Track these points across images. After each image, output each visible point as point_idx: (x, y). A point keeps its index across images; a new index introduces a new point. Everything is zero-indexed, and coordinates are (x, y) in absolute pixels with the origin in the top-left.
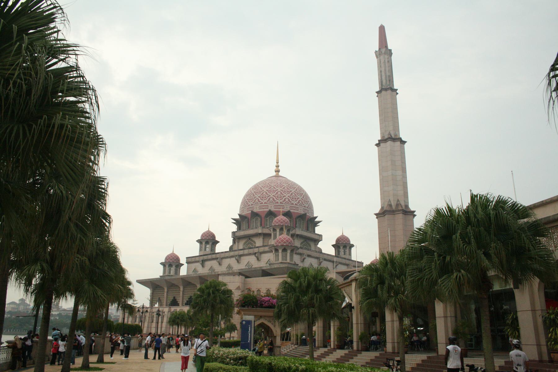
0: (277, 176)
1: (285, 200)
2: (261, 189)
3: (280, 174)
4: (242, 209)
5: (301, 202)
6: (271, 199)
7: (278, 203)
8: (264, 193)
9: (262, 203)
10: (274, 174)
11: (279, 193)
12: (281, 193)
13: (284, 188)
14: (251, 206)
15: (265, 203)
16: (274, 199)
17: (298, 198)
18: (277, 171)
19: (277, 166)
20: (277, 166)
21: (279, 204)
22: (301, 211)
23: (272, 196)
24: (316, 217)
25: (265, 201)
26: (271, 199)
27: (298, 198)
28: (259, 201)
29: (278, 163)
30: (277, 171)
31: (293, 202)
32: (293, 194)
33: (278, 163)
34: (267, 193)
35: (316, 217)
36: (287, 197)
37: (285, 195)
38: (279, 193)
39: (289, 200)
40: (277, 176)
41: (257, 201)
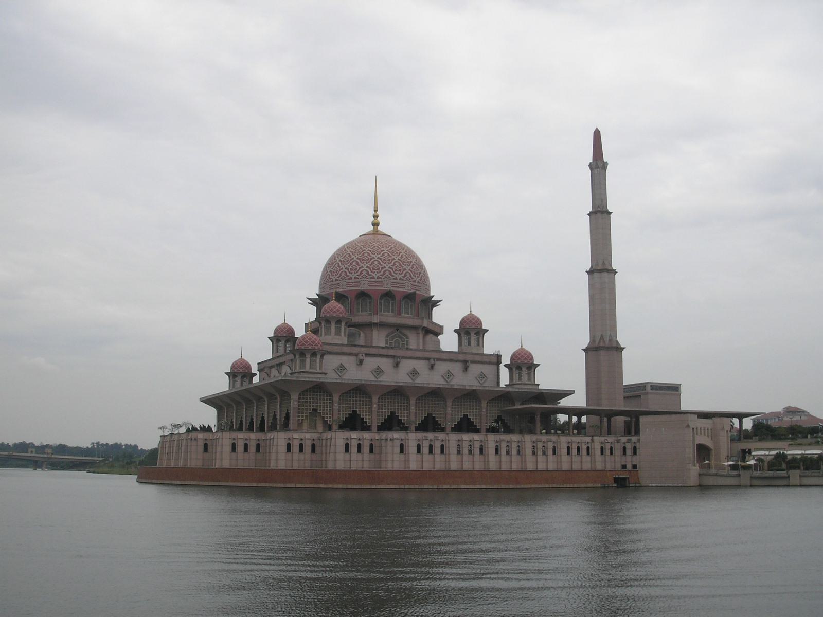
0: (376, 233)
1: (384, 273)
2: (350, 256)
3: (380, 228)
4: (322, 285)
6: (364, 273)
7: (373, 278)
8: (354, 263)
9: (351, 278)
10: (371, 228)
11: (376, 263)
12: (379, 263)
13: (383, 255)
14: (334, 283)
16: (368, 273)
17: (405, 269)
18: (375, 224)
19: (376, 217)
20: (376, 217)
22: (408, 289)
24: (433, 296)
25: (355, 275)
26: (364, 273)
27: (405, 269)
28: (346, 274)
29: (376, 211)
30: (375, 224)
32: (397, 264)
33: (376, 211)
34: (357, 263)
35: (433, 296)
36: (387, 268)
38: (376, 263)
40: (376, 233)
41: (343, 274)
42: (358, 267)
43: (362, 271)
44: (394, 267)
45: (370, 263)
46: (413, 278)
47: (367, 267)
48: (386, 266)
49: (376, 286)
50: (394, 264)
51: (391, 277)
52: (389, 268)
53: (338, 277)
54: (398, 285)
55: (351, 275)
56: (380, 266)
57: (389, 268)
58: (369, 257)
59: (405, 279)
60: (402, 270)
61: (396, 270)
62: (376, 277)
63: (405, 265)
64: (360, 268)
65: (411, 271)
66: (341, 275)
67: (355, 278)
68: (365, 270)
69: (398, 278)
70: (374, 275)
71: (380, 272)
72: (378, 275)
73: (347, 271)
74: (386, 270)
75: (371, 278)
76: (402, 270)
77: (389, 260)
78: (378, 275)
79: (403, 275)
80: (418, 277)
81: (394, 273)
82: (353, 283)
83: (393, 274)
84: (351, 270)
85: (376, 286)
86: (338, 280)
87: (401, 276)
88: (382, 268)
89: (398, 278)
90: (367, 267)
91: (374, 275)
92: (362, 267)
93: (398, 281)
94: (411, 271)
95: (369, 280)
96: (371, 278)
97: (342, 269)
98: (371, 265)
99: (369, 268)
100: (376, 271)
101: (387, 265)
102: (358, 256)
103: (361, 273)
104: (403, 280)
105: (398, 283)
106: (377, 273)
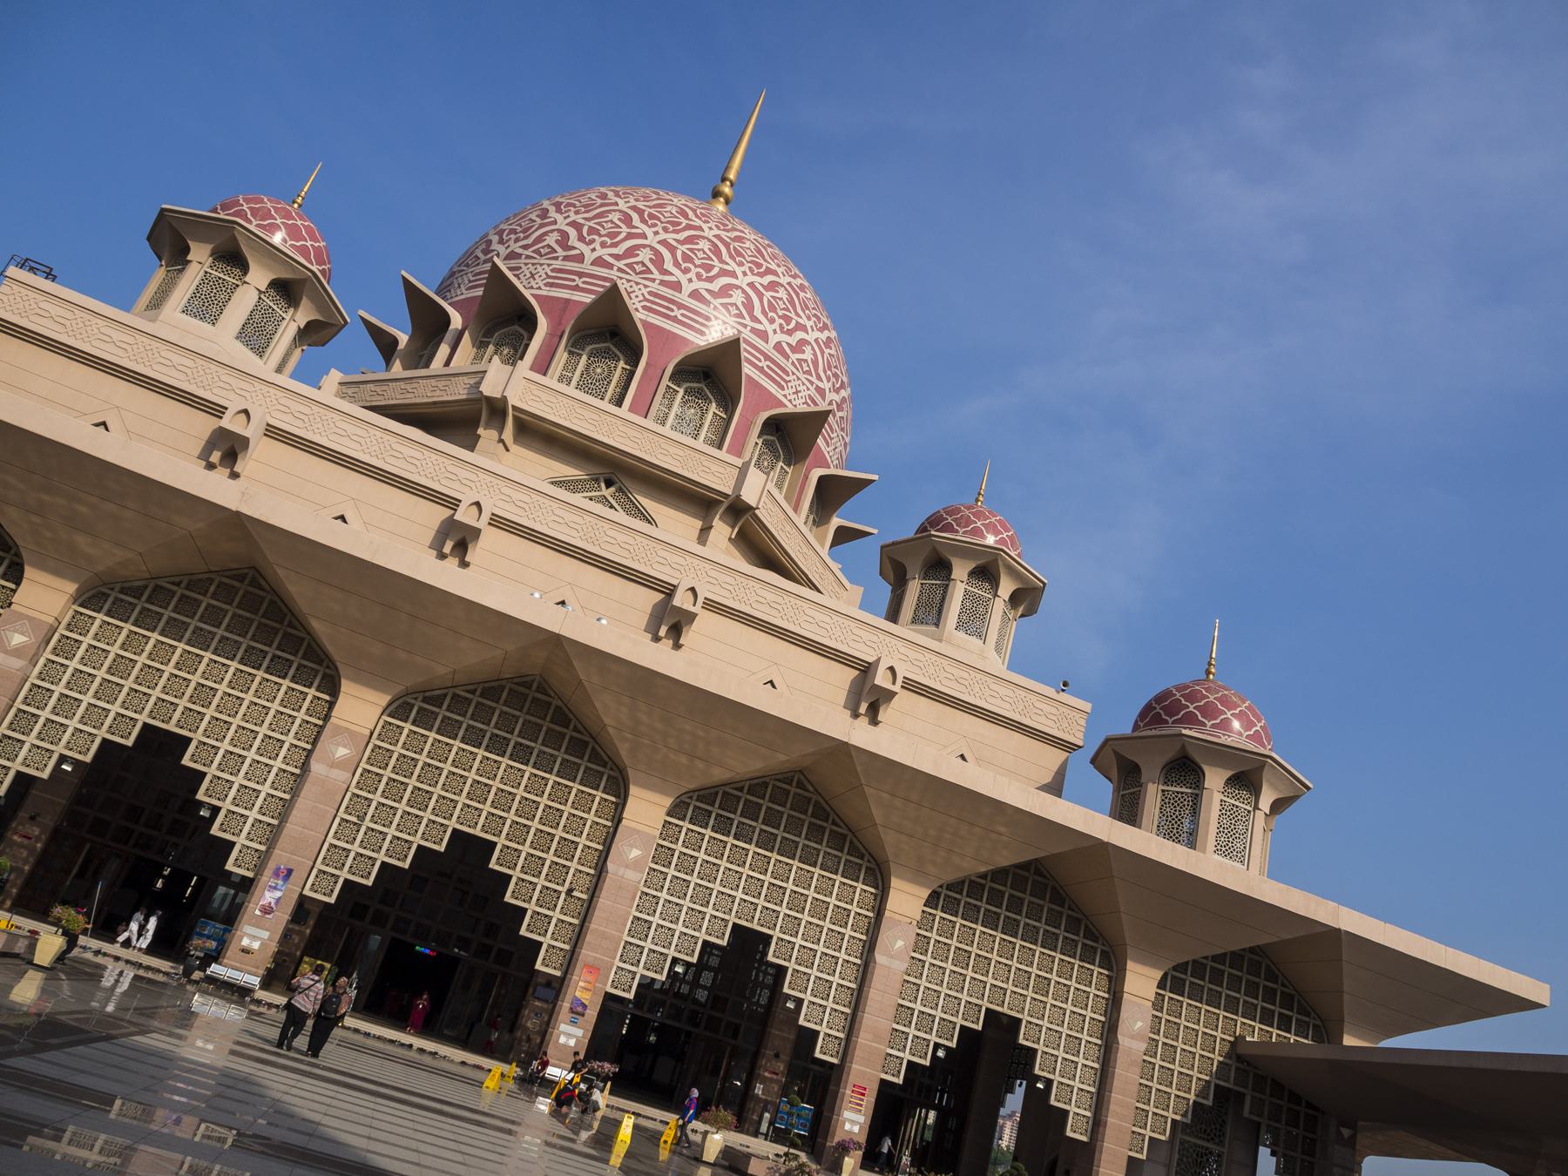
5: (808, 355)
6: (644, 256)
7: (677, 286)
8: (615, 217)
15: (599, 262)
16: (658, 260)
21: (683, 297)
22: (794, 400)
23: (652, 240)
25: (604, 253)
26: (644, 256)
28: (564, 241)
31: (769, 328)
34: (627, 220)
36: (743, 281)
37: (732, 266)
39: (749, 306)
41: (551, 240)
42: (625, 229)
43: (638, 247)
44: (768, 295)
45: (682, 236)
46: (819, 378)
47: (663, 242)
48: (740, 275)
49: (674, 319)
50: (772, 286)
51: (748, 321)
52: (751, 285)
53: (525, 247)
54: (764, 364)
55: (586, 249)
56: (716, 263)
57: (751, 285)
58: (685, 222)
59: (794, 357)
60: (793, 324)
61: (772, 308)
62: (687, 288)
63: (809, 318)
64: (630, 236)
65: (822, 353)
66: (539, 239)
67: (599, 262)
68: (652, 248)
69: (774, 339)
70: (683, 279)
71: (710, 280)
72: (697, 285)
73: (573, 233)
74: (737, 287)
75: (662, 283)
76: (793, 324)
77: (759, 266)
78: (697, 285)
79: (793, 340)
80: (837, 391)
81: (764, 313)
82: (581, 275)
83: (757, 312)
84: (592, 231)
85: (674, 319)
86: (519, 256)
87: (785, 338)
88: (724, 273)
89: (774, 339)
90: (663, 242)
91: (683, 279)
92: (644, 236)
93: (768, 348)
94: (822, 353)
95: (654, 287)
96: (662, 283)
97: (555, 222)
98: (682, 242)
99: (672, 250)
100: (694, 270)
101: (745, 274)
102: (640, 205)
103: (631, 252)
104: (787, 357)
105: (767, 358)
106: (699, 276)
